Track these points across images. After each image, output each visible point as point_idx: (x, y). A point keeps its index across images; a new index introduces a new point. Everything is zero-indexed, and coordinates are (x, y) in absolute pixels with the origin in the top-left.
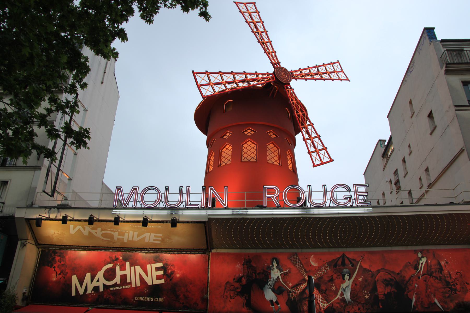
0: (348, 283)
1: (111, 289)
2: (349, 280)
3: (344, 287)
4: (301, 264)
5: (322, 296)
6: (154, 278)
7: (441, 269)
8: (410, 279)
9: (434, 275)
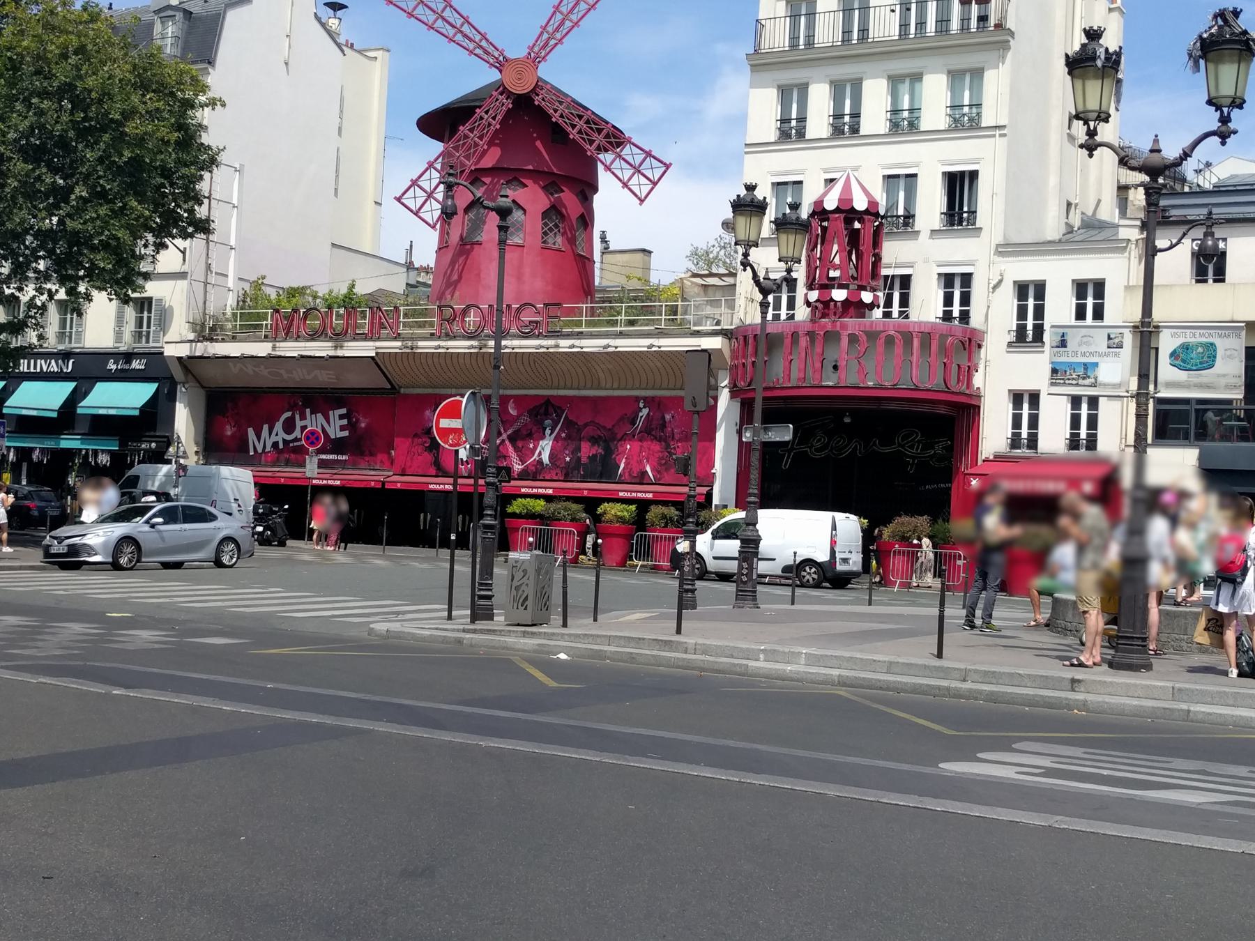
1: (291, 445)
5: (518, 456)
6: (338, 429)
7: (663, 425)
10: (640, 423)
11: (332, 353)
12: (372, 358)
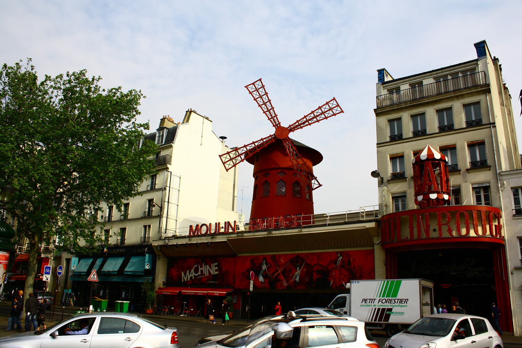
0: (298, 272)
1: (197, 278)
2: (299, 270)
3: (296, 274)
6: (214, 271)
10: (339, 263)
11: (210, 241)
12: (226, 241)
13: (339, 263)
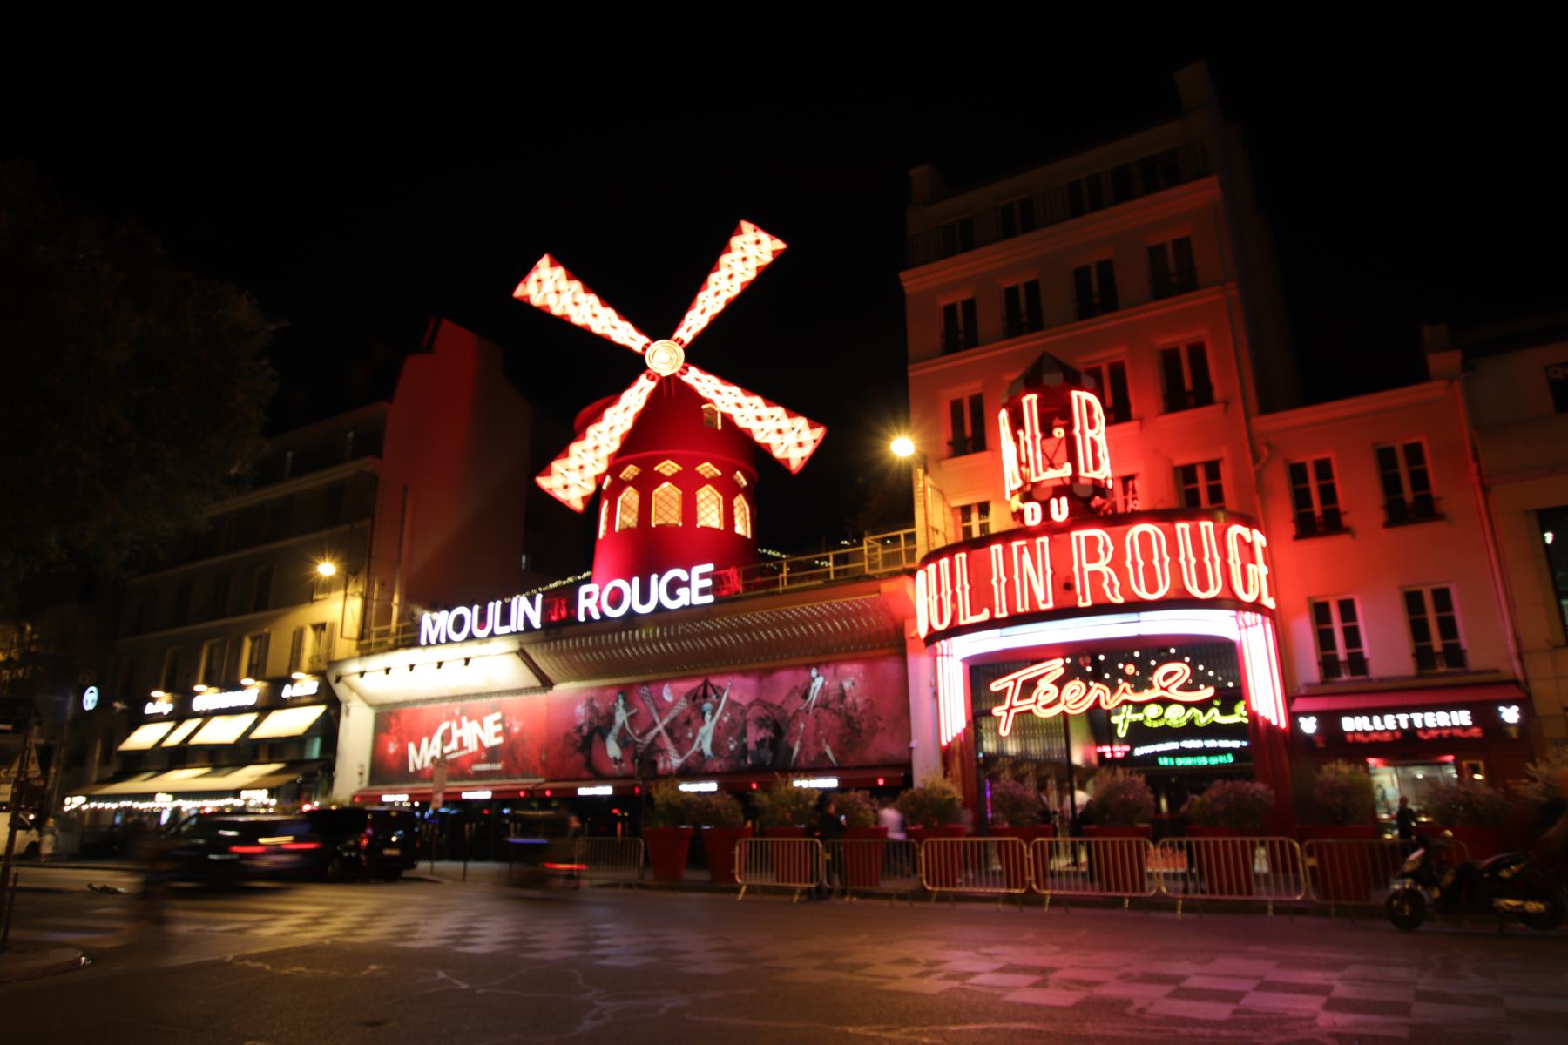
4: (652, 698)
5: (676, 748)
6: (492, 736)
7: (842, 695)
8: (795, 715)
9: (831, 706)
10: (814, 695)
13: (814, 695)
